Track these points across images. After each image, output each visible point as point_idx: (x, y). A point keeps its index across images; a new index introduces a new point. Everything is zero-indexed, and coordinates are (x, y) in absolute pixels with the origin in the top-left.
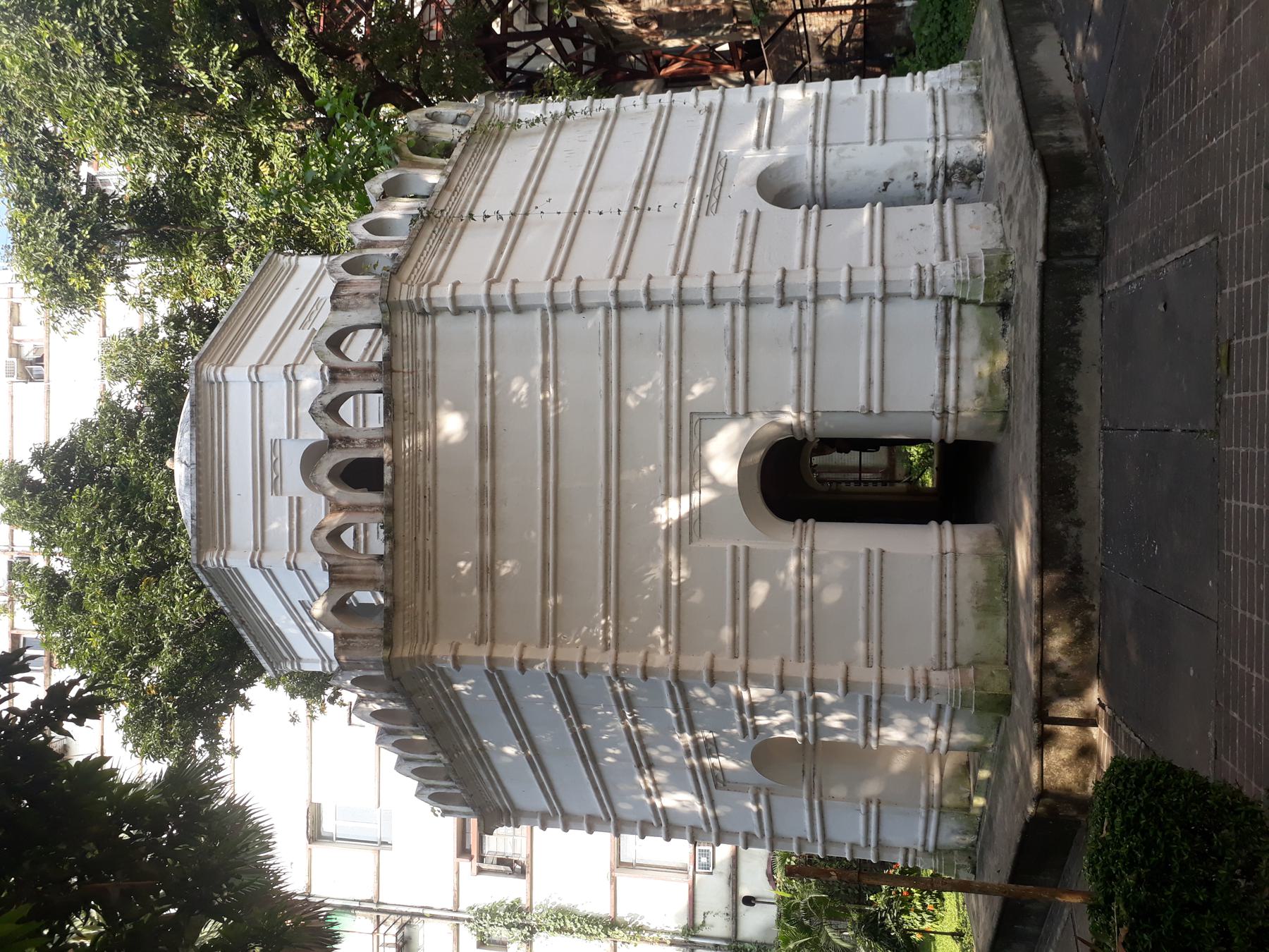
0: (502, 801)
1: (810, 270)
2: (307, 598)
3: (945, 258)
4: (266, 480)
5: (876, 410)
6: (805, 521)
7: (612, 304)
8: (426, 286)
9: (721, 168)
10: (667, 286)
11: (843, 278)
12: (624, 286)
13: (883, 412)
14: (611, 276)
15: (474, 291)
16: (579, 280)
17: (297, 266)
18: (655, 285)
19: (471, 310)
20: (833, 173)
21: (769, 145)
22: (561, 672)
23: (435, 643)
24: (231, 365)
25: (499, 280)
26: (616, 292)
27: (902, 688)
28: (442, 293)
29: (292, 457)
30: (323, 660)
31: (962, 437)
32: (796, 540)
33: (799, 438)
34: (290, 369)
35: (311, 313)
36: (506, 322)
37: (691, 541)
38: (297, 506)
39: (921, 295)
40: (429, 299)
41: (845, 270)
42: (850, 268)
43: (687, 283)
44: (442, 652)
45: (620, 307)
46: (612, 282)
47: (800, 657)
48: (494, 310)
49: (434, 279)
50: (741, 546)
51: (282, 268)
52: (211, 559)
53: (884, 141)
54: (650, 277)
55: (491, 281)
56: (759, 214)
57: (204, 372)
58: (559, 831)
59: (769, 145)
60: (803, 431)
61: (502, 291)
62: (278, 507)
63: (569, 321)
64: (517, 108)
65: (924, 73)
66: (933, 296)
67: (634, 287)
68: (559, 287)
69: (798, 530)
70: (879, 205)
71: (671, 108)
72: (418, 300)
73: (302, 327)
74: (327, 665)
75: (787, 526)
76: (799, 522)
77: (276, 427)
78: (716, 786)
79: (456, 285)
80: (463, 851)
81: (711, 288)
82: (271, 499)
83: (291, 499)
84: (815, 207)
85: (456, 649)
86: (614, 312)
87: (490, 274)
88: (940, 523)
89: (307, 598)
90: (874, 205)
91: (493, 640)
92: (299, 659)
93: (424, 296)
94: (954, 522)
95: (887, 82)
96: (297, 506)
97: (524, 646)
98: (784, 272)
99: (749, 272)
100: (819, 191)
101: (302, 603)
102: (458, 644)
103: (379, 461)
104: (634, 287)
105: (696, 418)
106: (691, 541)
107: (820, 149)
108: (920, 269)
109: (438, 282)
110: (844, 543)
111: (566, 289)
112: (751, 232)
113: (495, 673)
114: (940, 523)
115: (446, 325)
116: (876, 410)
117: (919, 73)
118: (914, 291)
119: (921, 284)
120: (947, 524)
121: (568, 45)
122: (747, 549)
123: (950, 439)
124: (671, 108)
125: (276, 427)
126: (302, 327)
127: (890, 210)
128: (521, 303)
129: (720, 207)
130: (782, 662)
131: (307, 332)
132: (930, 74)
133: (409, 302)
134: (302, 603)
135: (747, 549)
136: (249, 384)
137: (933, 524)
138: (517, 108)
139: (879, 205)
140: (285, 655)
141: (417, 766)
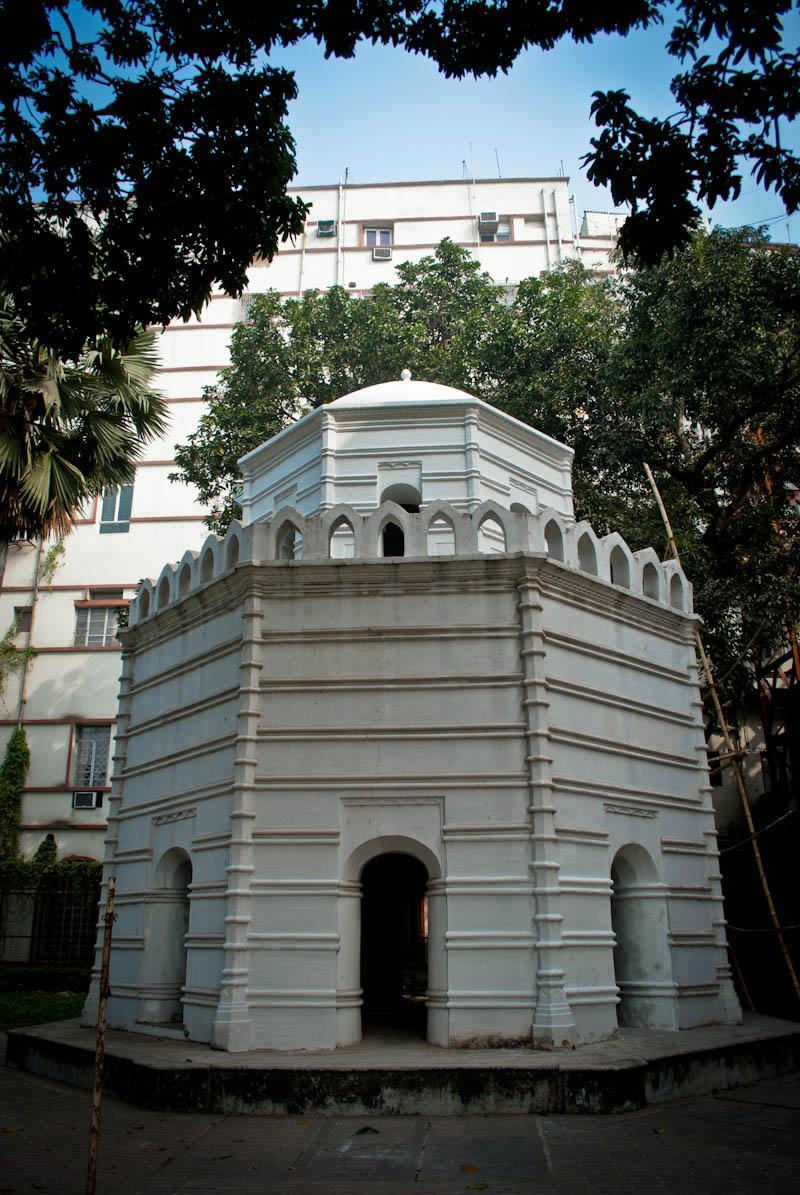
0: (141, 647)
1: (557, 889)
2: (300, 490)
3: (569, 995)
4: (389, 459)
5: (449, 944)
6: (362, 890)
7: (529, 732)
8: (538, 586)
9: (645, 814)
10: (544, 777)
11: (550, 916)
12: (543, 743)
13: (446, 950)
14: (551, 730)
15: (537, 623)
16: (546, 706)
17: (562, 471)
18: (544, 767)
19: (521, 622)
20: (646, 906)
21: (665, 852)
22: (241, 696)
23: (262, 598)
24: (479, 429)
25: (545, 641)
26: (537, 735)
27: (232, 966)
28: (533, 598)
29: (409, 478)
30: (252, 500)
31: (430, 1012)
32: (343, 883)
33: (428, 883)
34: (477, 475)
35: (522, 484)
36: (510, 648)
37: (342, 798)
38: (370, 482)
39: (539, 977)
40: (528, 588)
41: (558, 916)
42: (560, 921)
43: (547, 794)
44: (257, 605)
45: (527, 738)
46: (546, 732)
47: (253, 886)
48: (522, 638)
49: (544, 591)
50: (341, 839)
51: (559, 460)
52: (331, 419)
53: (672, 946)
54: (550, 762)
55: (546, 636)
56: (606, 846)
57: (472, 410)
58: (118, 692)
59: (665, 852)
60: (433, 887)
61: (537, 645)
62: (369, 468)
63: (512, 697)
64: (691, 645)
65: (731, 978)
66: (538, 988)
68: (540, 691)
69: (353, 884)
70: (615, 943)
71: (697, 770)
72: (528, 580)
73: (512, 480)
74: (248, 503)
75: (356, 876)
76: (360, 885)
77: (431, 465)
78: (153, 819)
79: (539, 608)
80: (97, 592)
81: (543, 811)
82: (376, 462)
83: (375, 477)
84: (612, 891)
85: (257, 615)
86: (522, 734)
87: (549, 634)
88: (361, 997)
89: (300, 489)
90: (615, 939)
91: (263, 692)
92: (252, 481)
93: (529, 585)
94: (362, 1008)
95: (723, 947)
96: (370, 482)
97: (260, 668)
98: (556, 869)
99: (555, 841)
100: (623, 896)
101: (296, 485)
102: (262, 617)
103: (401, 553)
105: (441, 801)
106: (342, 798)
107: (662, 894)
108: (560, 976)
109: (541, 594)
110: (344, 920)
111: (541, 696)
112: (591, 839)
114: (361, 997)
115: (506, 605)
116: (449, 944)
117: (730, 974)
118: (542, 972)
119: (548, 977)
120: (361, 1003)
121: (787, 666)
122: (337, 844)
123: (428, 1004)
124: (697, 770)
125: (431, 465)
126: (512, 480)
127: (611, 952)
128: (527, 659)
129: (611, 815)
130: (250, 873)
131: (507, 485)
132: (730, 983)
133: (525, 574)
134: (296, 485)
135: (337, 844)
136: (463, 443)
137: (360, 992)
138: (691, 645)
139: (615, 943)
140: (256, 471)
141: (171, 580)
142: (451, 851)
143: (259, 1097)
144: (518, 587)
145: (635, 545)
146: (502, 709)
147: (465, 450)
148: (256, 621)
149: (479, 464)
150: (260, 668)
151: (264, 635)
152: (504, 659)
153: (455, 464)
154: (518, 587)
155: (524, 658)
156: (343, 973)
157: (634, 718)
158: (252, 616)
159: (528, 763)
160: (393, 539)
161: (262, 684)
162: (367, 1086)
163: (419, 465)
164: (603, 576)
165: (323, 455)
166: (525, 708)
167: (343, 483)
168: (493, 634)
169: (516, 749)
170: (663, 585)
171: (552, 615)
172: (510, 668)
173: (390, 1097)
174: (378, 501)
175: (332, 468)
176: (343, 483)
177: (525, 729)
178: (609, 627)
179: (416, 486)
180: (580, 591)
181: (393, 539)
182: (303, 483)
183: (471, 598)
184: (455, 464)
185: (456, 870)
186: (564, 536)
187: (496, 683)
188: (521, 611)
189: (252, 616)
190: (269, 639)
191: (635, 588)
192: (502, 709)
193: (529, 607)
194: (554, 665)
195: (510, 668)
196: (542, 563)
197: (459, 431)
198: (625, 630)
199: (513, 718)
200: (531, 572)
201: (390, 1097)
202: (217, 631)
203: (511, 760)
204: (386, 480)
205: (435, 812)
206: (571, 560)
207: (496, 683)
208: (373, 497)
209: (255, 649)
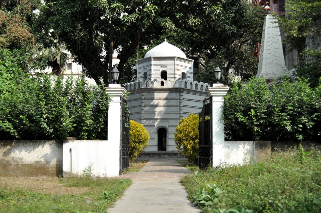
4: (162, 65)
15: (182, 97)
28: (182, 94)
29: (165, 69)
38: (159, 70)
48: (180, 100)
62: (159, 67)
67: (182, 115)
77: (169, 67)
96: (159, 70)
97: (144, 103)
104: (182, 115)
110: (156, 136)
113: (140, 99)
125: (169, 67)
134: (146, 68)
142: (170, 128)
143: (146, 156)
144: (180, 92)
145: (199, 82)
146: (177, 109)
147: (174, 65)
148: (143, 96)
149: (176, 67)
150: (144, 103)
151: (144, 98)
152: (177, 102)
153: (172, 67)
154: (180, 92)
155: (180, 102)
156: (155, 142)
157: (197, 109)
158: (142, 95)
159: (180, 117)
160: (162, 84)
161: (144, 105)
162: (159, 154)
163: (167, 67)
164: (194, 88)
165: (151, 65)
166: (180, 109)
167: (155, 70)
168: (176, 99)
169: (178, 115)
170: (204, 88)
171: (185, 96)
172: (178, 104)
173: (161, 155)
174: (160, 73)
175: (153, 67)
176: (155, 70)
177: (180, 112)
178: (194, 96)
179: (166, 70)
180: (190, 91)
181: (162, 84)
182: (148, 68)
183: (174, 93)
184: (172, 67)
185: (170, 130)
186: (187, 83)
187: (176, 106)
188: (180, 96)
189: (142, 95)
190: (145, 99)
191: (199, 89)
192: (177, 109)
193: (181, 95)
194: (185, 103)
195: (178, 104)
196: (183, 89)
197: (173, 61)
198: (197, 96)
199: (178, 111)
200: (182, 90)
201: (161, 155)
202: (137, 96)
203: (178, 116)
204: (162, 69)
205: (168, 123)
206: (189, 87)
207: (176, 106)
208: (160, 72)
209: (143, 100)
